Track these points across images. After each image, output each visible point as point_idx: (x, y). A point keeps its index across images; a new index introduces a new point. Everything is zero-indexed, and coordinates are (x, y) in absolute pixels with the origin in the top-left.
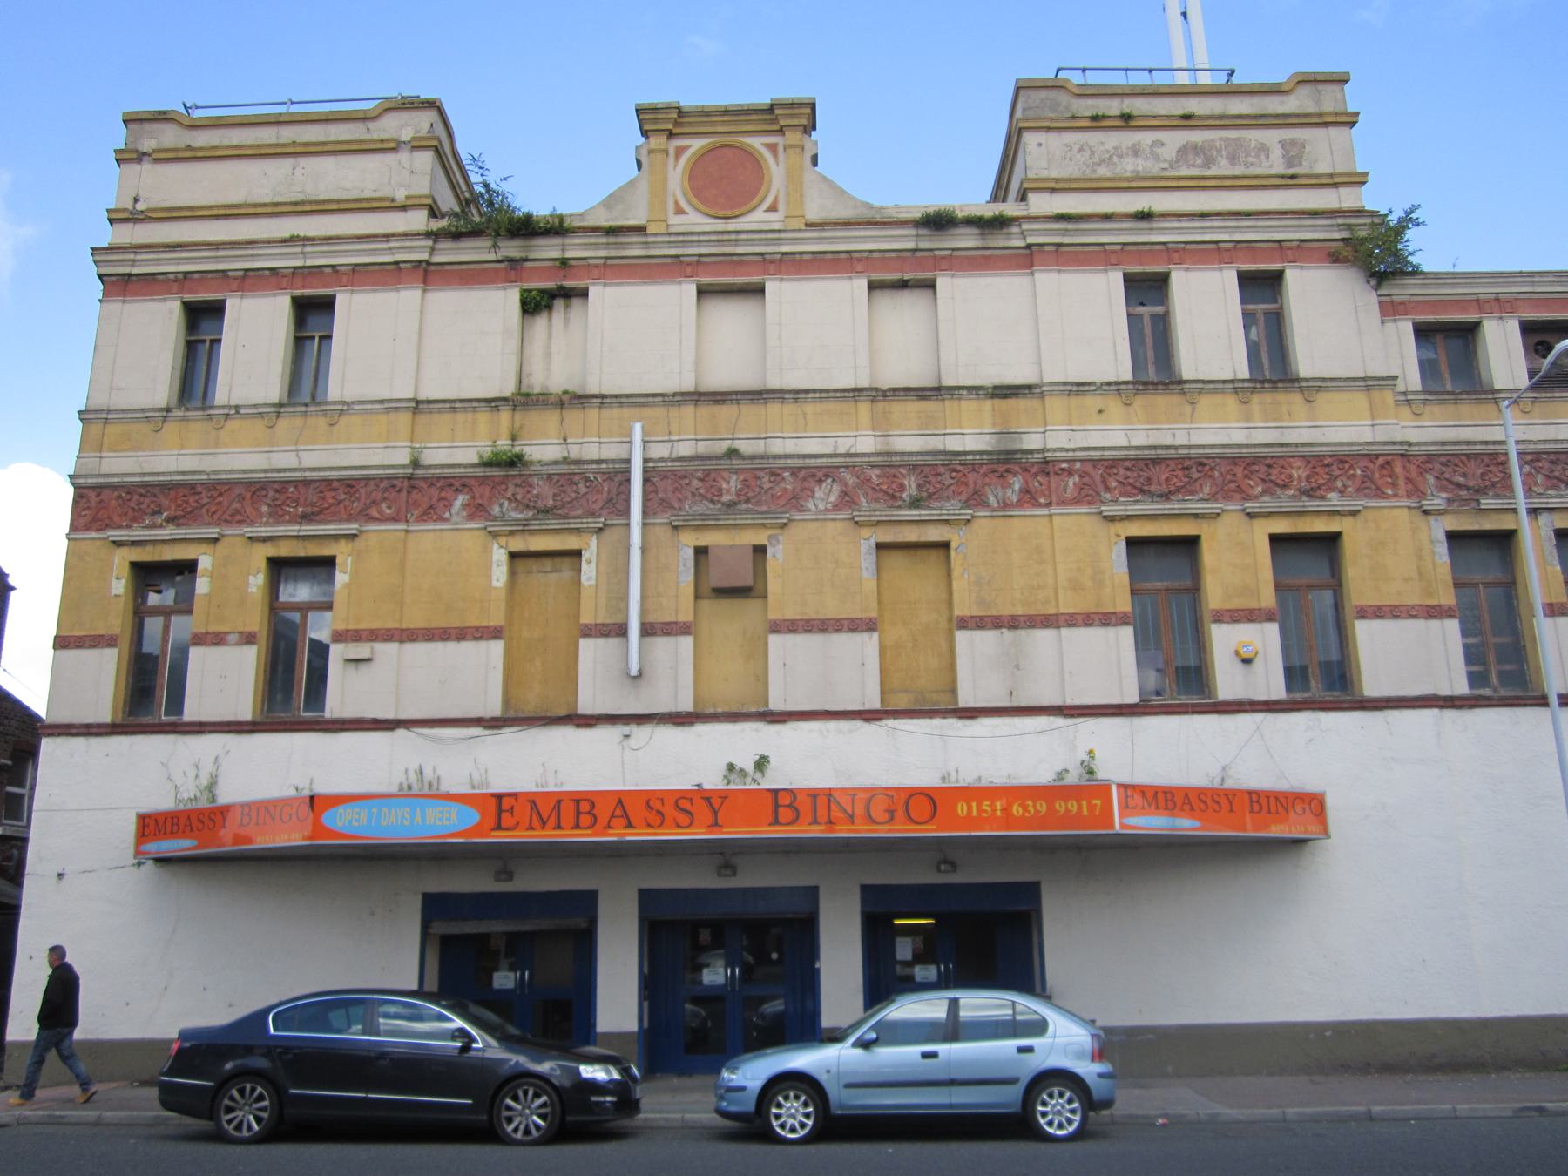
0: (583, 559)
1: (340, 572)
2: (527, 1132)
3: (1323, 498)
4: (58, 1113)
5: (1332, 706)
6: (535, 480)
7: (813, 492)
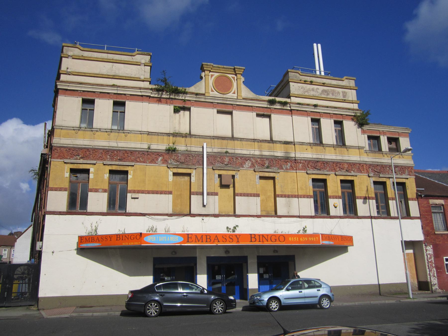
0: (192, 176)
1: (129, 174)
2: (219, 311)
3: (350, 172)
4: (81, 314)
5: (352, 218)
6: (179, 155)
7: (245, 163)
